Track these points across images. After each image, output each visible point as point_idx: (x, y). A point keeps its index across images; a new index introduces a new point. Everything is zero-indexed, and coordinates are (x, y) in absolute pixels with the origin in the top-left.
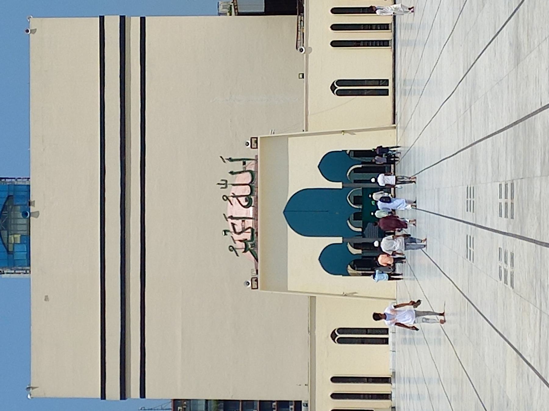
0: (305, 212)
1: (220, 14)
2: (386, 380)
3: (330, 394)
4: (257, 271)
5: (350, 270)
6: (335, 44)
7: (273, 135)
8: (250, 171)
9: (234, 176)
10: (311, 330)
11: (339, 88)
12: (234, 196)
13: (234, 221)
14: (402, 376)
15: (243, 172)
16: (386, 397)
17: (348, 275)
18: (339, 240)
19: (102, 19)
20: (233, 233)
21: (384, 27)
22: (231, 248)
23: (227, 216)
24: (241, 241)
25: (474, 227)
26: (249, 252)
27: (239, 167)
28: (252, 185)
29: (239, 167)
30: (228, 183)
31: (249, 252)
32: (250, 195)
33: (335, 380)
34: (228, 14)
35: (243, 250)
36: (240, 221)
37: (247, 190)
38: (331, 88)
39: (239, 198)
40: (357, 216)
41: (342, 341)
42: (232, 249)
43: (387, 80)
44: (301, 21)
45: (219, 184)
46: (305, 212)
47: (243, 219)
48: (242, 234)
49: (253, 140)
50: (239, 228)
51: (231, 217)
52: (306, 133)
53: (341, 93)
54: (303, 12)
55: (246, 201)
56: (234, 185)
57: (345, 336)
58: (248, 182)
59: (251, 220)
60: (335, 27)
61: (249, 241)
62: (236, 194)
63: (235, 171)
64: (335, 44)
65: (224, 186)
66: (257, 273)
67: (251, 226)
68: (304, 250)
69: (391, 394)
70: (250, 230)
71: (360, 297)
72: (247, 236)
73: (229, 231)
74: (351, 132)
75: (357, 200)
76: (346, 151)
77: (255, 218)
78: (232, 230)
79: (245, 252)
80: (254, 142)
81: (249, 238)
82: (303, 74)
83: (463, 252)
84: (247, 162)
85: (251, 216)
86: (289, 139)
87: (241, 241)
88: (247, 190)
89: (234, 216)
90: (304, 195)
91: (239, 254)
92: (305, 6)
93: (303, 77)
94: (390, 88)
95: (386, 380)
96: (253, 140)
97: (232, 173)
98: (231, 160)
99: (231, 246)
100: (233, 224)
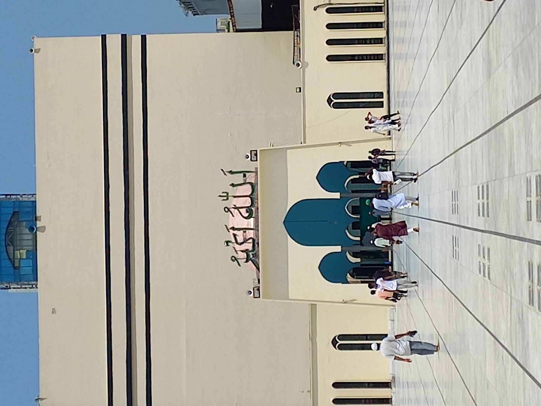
0: (304, 223)
1: (218, 31)
2: (386, 385)
3: (332, 399)
4: (259, 280)
5: (349, 278)
7: (272, 148)
9: (235, 188)
10: (313, 337)
11: (335, 101)
12: (235, 208)
13: (235, 232)
14: (401, 381)
15: (243, 184)
17: (348, 283)
18: (338, 249)
19: (104, 38)
20: (235, 244)
21: (378, 41)
22: (233, 258)
23: (229, 227)
24: (242, 251)
25: (458, 228)
27: (239, 179)
28: (252, 197)
29: (239, 179)
30: (229, 195)
32: (250, 206)
33: (336, 385)
34: (226, 30)
35: (245, 260)
36: (242, 231)
37: (247, 202)
38: (328, 101)
39: (241, 210)
40: (356, 226)
41: (342, 347)
42: (234, 259)
43: (382, 93)
44: (297, 36)
45: (220, 196)
46: (304, 223)
47: (245, 230)
48: (243, 245)
49: (253, 153)
50: (240, 239)
51: (233, 228)
52: (304, 145)
54: (299, 28)
55: (247, 212)
56: (235, 197)
58: (248, 194)
59: (252, 231)
60: (330, 42)
61: (251, 251)
62: (237, 206)
63: (235, 183)
64: (330, 58)
65: (225, 198)
66: (259, 283)
67: (253, 237)
68: (305, 260)
69: (391, 399)
70: (251, 241)
72: (249, 246)
73: (230, 242)
74: (348, 144)
75: (355, 210)
76: (343, 162)
77: (256, 229)
78: (234, 241)
79: (247, 262)
80: (254, 155)
82: (300, 88)
83: (450, 253)
84: (247, 174)
85: (252, 227)
86: (288, 151)
87: (242, 251)
88: (247, 202)
89: (236, 227)
90: (303, 205)
91: (241, 264)
92: (301, 22)
93: (300, 91)
94: (385, 100)
95: (386, 385)
96: (253, 153)
97: (233, 185)
98: (231, 172)
99: (233, 257)
100: (235, 235)
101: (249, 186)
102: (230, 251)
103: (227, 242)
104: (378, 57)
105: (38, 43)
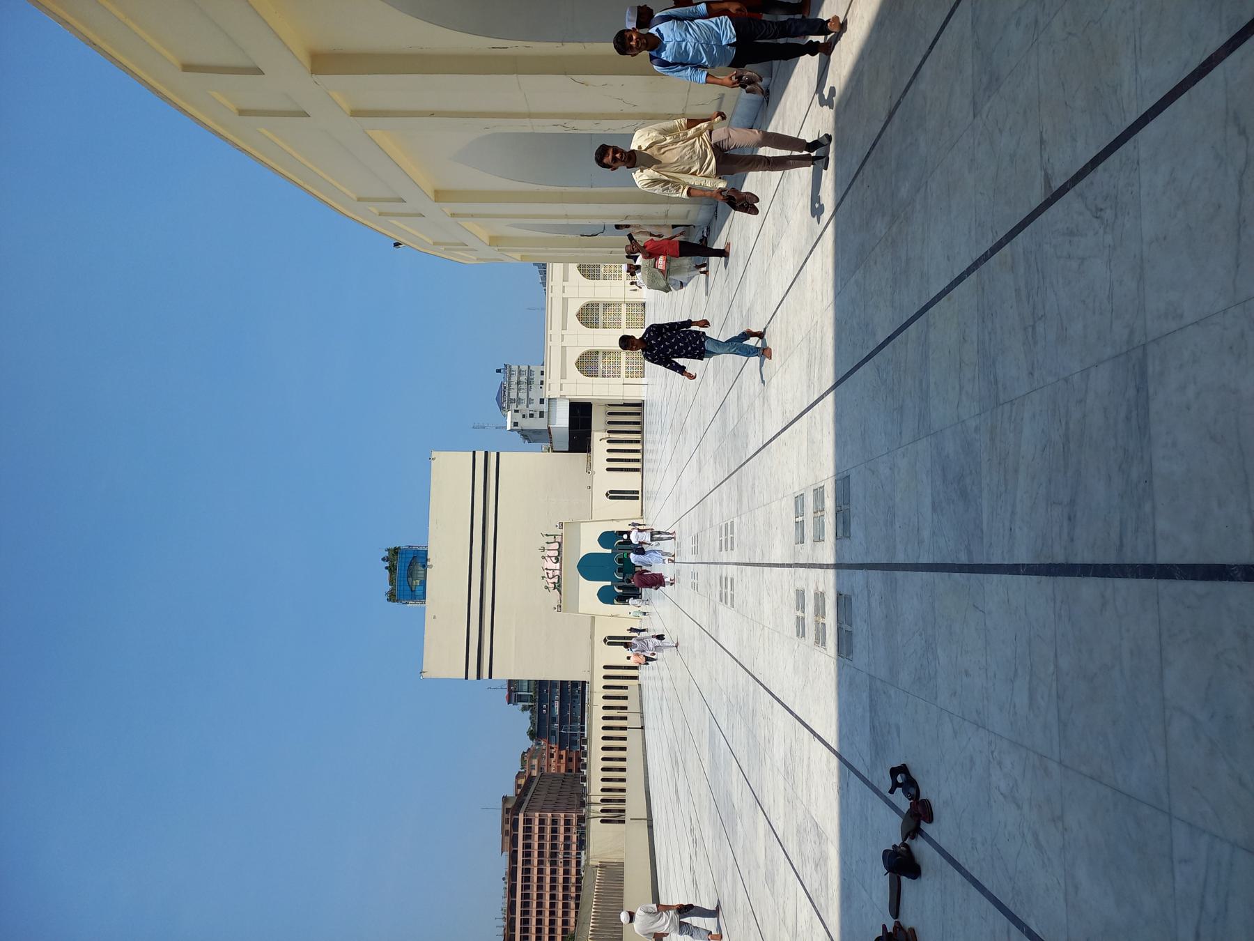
6: (608, 469)
10: (592, 637)
16: (635, 678)
18: (609, 583)
27: (552, 539)
28: (559, 551)
29: (552, 539)
33: (605, 667)
37: (556, 553)
40: (620, 570)
46: (589, 567)
53: (611, 498)
57: (611, 641)
68: (590, 589)
71: (621, 617)
72: (556, 580)
75: (620, 561)
90: (589, 557)
102: (544, 583)
104: (637, 470)
105: (434, 454)
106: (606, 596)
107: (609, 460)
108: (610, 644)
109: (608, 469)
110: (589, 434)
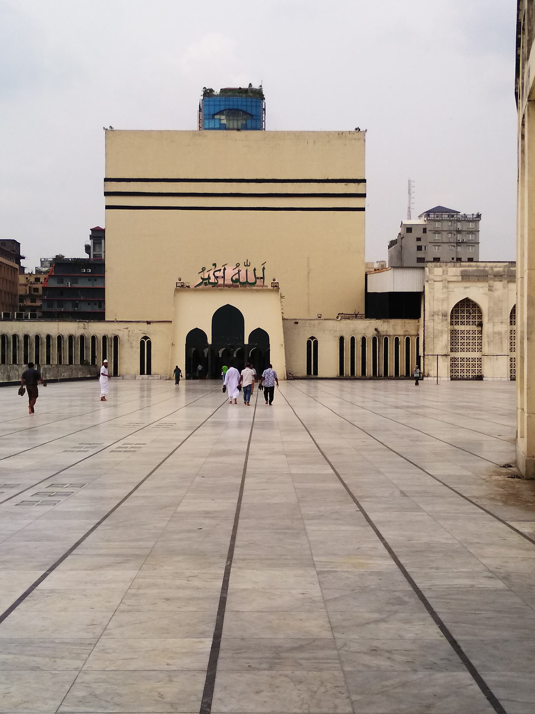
0: (228, 319)
6: (342, 339)
8: (256, 282)
12: (239, 271)
13: (222, 271)
18: (210, 341)
26: (201, 281)
27: (259, 274)
31: (201, 281)
42: (203, 269)
46: (228, 319)
47: (224, 277)
51: (225, 269)
53: (309, 343)
56: (247, 271)
57: (146, 346)
70: (216, 281)
72: (212, 280)
73: (215, 267)
77: (224, 285)
78: (216, 269)
81: (210, 281)
84: (262, 280)
97: (255, 270)
98: (264, 269)
100: (220, 270)
101: (254, 281)
102: (209, 266)
103: (215, 265)
106: (195, 337)
107: (353, 339)
108: (142, 343)
109: (342, 339)
110: (378, 316)
